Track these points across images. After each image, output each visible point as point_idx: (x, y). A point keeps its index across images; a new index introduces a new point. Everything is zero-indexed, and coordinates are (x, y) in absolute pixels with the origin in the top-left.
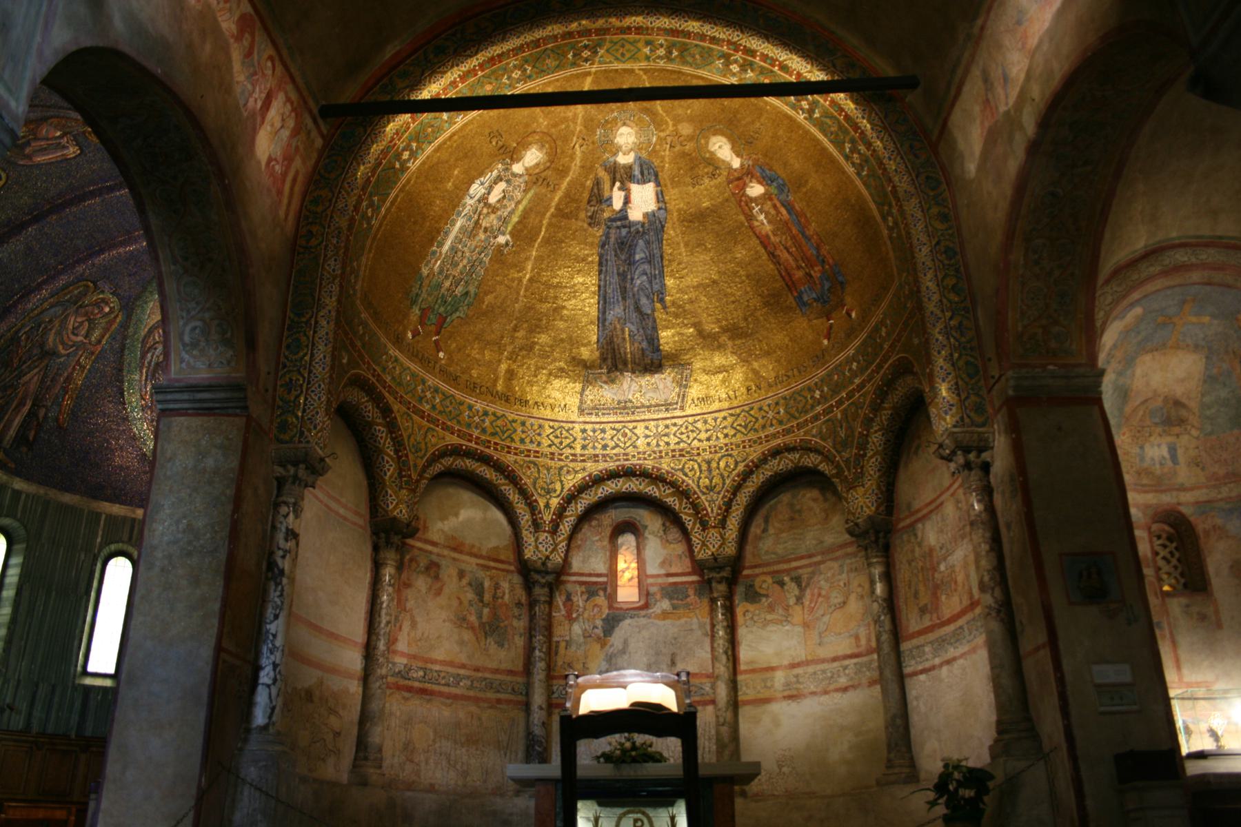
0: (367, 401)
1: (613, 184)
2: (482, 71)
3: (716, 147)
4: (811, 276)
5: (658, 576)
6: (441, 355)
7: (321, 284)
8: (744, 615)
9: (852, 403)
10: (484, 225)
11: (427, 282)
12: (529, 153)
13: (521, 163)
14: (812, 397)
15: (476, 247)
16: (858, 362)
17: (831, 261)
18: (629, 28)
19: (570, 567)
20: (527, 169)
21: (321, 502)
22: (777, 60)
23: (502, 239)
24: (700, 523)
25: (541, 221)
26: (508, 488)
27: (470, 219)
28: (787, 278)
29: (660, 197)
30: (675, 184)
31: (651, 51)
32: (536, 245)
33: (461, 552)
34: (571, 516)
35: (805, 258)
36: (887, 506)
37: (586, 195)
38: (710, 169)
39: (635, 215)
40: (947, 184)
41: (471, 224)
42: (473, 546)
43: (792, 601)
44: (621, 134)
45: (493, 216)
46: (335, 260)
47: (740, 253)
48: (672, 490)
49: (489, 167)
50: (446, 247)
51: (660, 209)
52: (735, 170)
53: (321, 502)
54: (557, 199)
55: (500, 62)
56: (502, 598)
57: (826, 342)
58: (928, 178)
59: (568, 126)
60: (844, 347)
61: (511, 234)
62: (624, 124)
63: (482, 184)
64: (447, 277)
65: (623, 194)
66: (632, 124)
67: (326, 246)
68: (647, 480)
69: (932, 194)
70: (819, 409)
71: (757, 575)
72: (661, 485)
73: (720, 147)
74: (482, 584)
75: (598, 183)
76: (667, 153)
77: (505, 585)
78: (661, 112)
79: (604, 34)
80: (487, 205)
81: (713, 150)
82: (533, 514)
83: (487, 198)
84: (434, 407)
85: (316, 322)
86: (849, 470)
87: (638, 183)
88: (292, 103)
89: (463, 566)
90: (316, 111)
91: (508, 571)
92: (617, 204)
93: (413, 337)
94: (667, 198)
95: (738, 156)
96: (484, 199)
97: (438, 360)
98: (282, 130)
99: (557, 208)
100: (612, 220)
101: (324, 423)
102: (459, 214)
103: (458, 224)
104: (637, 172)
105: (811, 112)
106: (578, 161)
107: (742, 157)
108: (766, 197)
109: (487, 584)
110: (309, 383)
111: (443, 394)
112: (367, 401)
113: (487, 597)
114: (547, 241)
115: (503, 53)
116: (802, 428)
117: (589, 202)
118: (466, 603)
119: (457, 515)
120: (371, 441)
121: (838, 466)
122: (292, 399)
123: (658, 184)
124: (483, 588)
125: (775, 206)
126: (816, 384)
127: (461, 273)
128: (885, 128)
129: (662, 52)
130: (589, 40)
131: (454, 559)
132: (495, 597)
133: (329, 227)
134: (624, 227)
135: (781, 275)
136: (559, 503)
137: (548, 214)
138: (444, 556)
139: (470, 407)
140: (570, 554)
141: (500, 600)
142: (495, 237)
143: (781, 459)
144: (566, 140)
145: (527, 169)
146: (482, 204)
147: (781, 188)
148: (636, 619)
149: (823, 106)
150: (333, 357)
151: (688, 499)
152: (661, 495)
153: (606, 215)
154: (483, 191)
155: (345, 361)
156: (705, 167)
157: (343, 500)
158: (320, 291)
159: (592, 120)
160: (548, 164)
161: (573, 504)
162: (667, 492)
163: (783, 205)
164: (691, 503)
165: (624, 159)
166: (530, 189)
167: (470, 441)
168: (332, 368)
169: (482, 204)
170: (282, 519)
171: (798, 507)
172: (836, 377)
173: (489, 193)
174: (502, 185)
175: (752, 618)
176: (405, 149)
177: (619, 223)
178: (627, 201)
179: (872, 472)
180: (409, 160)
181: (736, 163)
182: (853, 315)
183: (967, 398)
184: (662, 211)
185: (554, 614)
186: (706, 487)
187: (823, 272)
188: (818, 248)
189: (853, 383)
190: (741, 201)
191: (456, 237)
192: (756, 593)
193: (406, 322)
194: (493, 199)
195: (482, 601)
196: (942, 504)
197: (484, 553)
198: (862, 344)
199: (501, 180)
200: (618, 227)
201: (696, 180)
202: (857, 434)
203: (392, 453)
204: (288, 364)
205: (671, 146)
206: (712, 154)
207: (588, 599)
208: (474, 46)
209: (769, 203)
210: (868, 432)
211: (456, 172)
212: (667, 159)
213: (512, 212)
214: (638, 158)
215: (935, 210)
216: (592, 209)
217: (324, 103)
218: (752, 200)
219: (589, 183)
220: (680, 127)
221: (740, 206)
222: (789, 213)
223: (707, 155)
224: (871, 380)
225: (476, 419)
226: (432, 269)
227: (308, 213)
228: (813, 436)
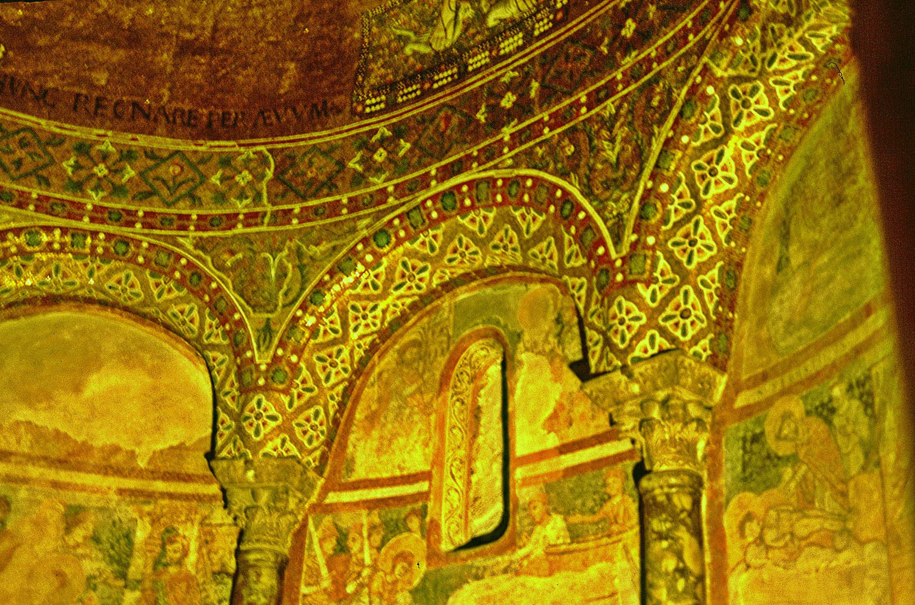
5: (541, 456)
8: (741, 528)
19: (350, 470)
26: (187, 308)
33: (79, 468)
42: (116, 449)
43: (855, 460)
56: (180, 563)
71: (769, 402)
74: (128, 537)
77: (191, 533)
89: (80, 498)
91: (200, 498)
109: (140, 535)
113: (138, 565)
118: (77, 584)
124: (130, 543)
131: (56, 485)
132: (159, 563)
138: (25, 481)
140: (352, 438)
141: (172, 570)
148: (487, 580)
175: (760, 540)
185: (304, 590)
192: (769, 457)
195: (123, 576)
197: (142, 464)
207: (383, 543)
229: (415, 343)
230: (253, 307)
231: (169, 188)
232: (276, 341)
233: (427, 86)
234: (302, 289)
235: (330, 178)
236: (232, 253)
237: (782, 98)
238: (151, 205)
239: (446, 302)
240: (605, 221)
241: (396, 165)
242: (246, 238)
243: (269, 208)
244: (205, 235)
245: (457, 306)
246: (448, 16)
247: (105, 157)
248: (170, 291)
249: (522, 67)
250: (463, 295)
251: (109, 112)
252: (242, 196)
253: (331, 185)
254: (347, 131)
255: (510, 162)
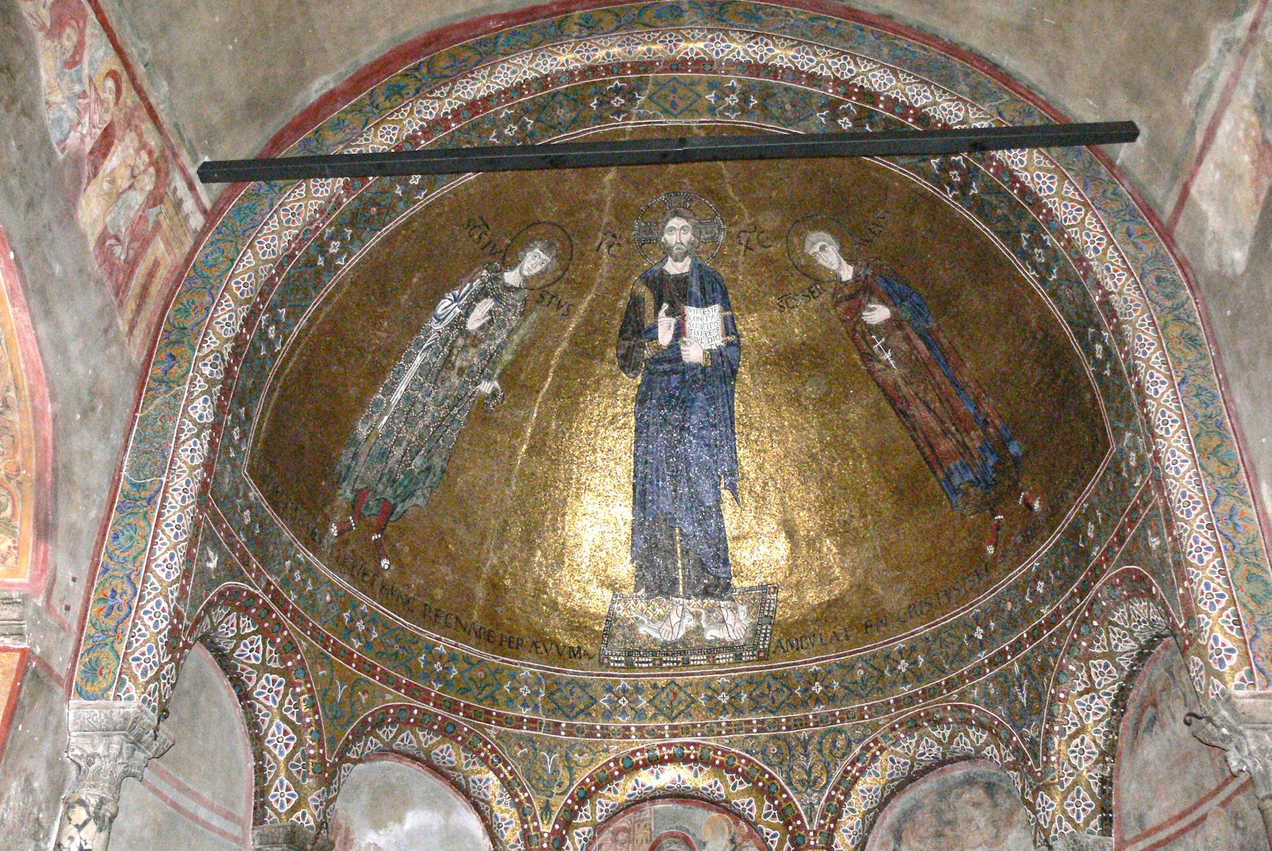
0: (254, 633)
1: (658, 308)
2: (458, 122)
3: (817, 248)
4: (964, 445)
6: (385, 563)
7: (178, 438)
9: (1038, 647)
10: (458, 364)
11: (364, 449)
12: (529, 255)
13: (517, 270)
14: (971, 637)
15: (446, 397)
16: (1047, 582)
17: (997, 422)
18: (684, 61)
20: (525, 279)
21: (164, 798)
22: (911, 107)
23: (486, 387)
24: (792, 841)
25: (547, 361)
27: (436, 354)
28: (927, 450)
29: (729, 327)
30: (753, 304)
31: (718, 98)
32: (539, 400)
34: (584, 825)
35: (958, 420)
36: (1103, 820)
37: (617, 322)
38: (806, 283)
39: (693, 353)
40: (1191, 288)
41: (438, 361)
44: (672, 229)
45: (472, 351)
46: (205, 401)
47: (855, 414)
48: (746, 785)
49: (469, 274)
50: (398, 395)
51: (729, 344)
52: (846, 283)
53: (164, 798)
54: (573, 326)
55: (485, 109)
57: (990, 550)
58: (1159, 279)
59: (590, 215)
60: (1021, 557)
61: (500, 378)
62: (676, 214)
63: (456, 299)
64: (398, 442)
65: (673, 321)
66: (686, 213)
67: (194, 378)
68: (706, 769)
69: (1169, 304)
70: (983, 656)
72: (728, 776)
73: (822, 248)
75: (636, 302)
76: (741, 258)
78: (732, 194)
79: (645, 71)
80: (464, 333)
81: (810, 253)
82: (524, 821)
83: (464, 323)
84: (368, 645)
85: (164, 499)
86: (1035, 757)
87: (697, 306)
88: (150, 153)
90: (193, 171)
92: (665, 336)
93: (340, 533)
94: (740, 327)
95: (849, 262)
96: (459, 324)
97: (379, 570)
98: (132, 193)
99: (574, 342)
100: (656, 361)
101: (162, 667)
102: (419, 345)
103: (418, 361)
104: (695, 289)
105: (964, 187)
106: (604, 270)
107: (856, 264)
108: (895, 323)
110: (141, 598)
111: (385, 626)
112: (254, 633)
114: (556, 393)
115: (490, 95)
116: (954, 687)
117: (622, 332)
119: (400, 820)
120: (261, 698)
121: (1017, 749)
122: (113, 624)
123: (726, 306)
125: (907, 338)
126: (976, 618)
127: (421, 437)
128: (1085, 204)
129: (732, 100)
130: (622, 80)
133: (201, 347)
134: (673, 372)
135: (918, 446)
136: (566, 804)
137: (558, 352)
139: (430, 648)
142: (476, 385)
143: (921, 738)
144: (585, 236)
145: (525, 279)
146: (456, 332)
147: (917, 311)
149: (984, 175)
150: (189, 557)
151: (772, 799)
152: (728, 793)
153: (647, 353)
154: (458, 310)
155: (212, 565)
156: (798, 281)
157: (206, 795)
158: (176, 448)
159: (626, 207)
160: (559, 273)
161: (588, 806)
162: (739, 788)
163: (921, 336)
164: (776, 808)
165: (674, 268)
166: (531, 311)
167: (426, 701)
168: (186, 575)
169: (456, 332)
170: (74, 832)
171: (949, 816)
172: (1009, 605)
173: (467, 315)
174: (487, 305)
176: (332, 238)
177: (667, 367)
178: (680, 332)
179: (1075, 762)
180: (339, 255)
181: (847, 273)
182: (1037, 505)
183: (1255, 637)
184: (733, 348)
186: (802, 782)
187: (986, 438)
188: (977, 402)
189: (1039, 614)
190: (854, 330)
191: (414, 380)
193: (327, 510)
194: (473, 324)
196: (1203, 818)
198: (1052, 552)
199: (486, 296)
200: (665, 373)
201: (784, 302)
202: (1048, 698)
203: (294, 719)
204: (111, 565)
205: (746, 247)
206: (812, 259)
208: (445, 84)
209: (899, 333)
210: (1067, 694)
211: (415, 280)
212: (741, 269)
213: (501, 347)
214: (697, 266)
215: (1175, 331)
216: (627, 344)
217: (207, 159)
218: (872, 329)
219: (622, 304)
220: (760, 218)
221: (853, 339)
222: (930, 348)
223: (803, 262)
224: (1069, 610)
225: (438, 666)
226: (373, 428)
227: (169, 328)
228: (974, 701)
229: (624, 829)
230: (537, 790)
231: (478, 688)
232: (554, 818)
233: (657, 662)
234: (571, 784)
235: (587, 707)
236: (521, 748)
237: (915, 769)
238: (467, 698)
239: (647, 806)
240: (802, 805)
241: (640, 715)
242: (530, 740)
243: (544, 719)
244: (503, 729)
245: (656, 812)
246: (675, 619)
247: (441, 657)
248: (474, 763)
249: (734, 679)
250: (659, 806)
251: (442, 621)
252: (525, 705)
253: (586, 712)
254: (597, 675)
255: (727, 741)
